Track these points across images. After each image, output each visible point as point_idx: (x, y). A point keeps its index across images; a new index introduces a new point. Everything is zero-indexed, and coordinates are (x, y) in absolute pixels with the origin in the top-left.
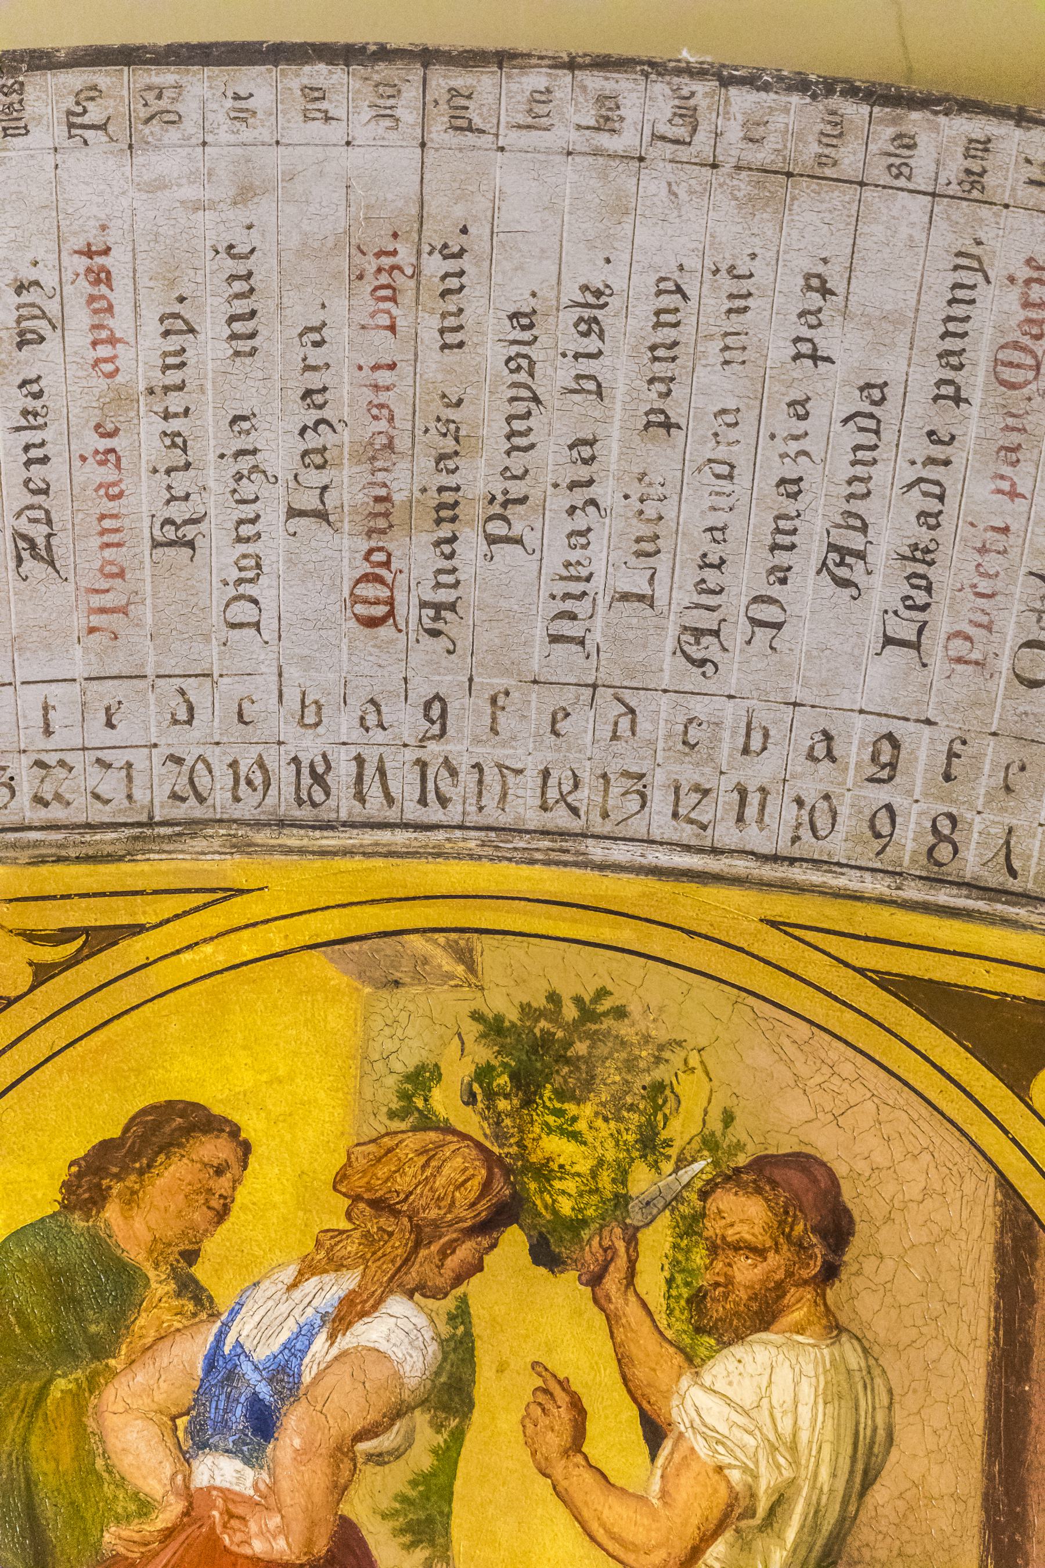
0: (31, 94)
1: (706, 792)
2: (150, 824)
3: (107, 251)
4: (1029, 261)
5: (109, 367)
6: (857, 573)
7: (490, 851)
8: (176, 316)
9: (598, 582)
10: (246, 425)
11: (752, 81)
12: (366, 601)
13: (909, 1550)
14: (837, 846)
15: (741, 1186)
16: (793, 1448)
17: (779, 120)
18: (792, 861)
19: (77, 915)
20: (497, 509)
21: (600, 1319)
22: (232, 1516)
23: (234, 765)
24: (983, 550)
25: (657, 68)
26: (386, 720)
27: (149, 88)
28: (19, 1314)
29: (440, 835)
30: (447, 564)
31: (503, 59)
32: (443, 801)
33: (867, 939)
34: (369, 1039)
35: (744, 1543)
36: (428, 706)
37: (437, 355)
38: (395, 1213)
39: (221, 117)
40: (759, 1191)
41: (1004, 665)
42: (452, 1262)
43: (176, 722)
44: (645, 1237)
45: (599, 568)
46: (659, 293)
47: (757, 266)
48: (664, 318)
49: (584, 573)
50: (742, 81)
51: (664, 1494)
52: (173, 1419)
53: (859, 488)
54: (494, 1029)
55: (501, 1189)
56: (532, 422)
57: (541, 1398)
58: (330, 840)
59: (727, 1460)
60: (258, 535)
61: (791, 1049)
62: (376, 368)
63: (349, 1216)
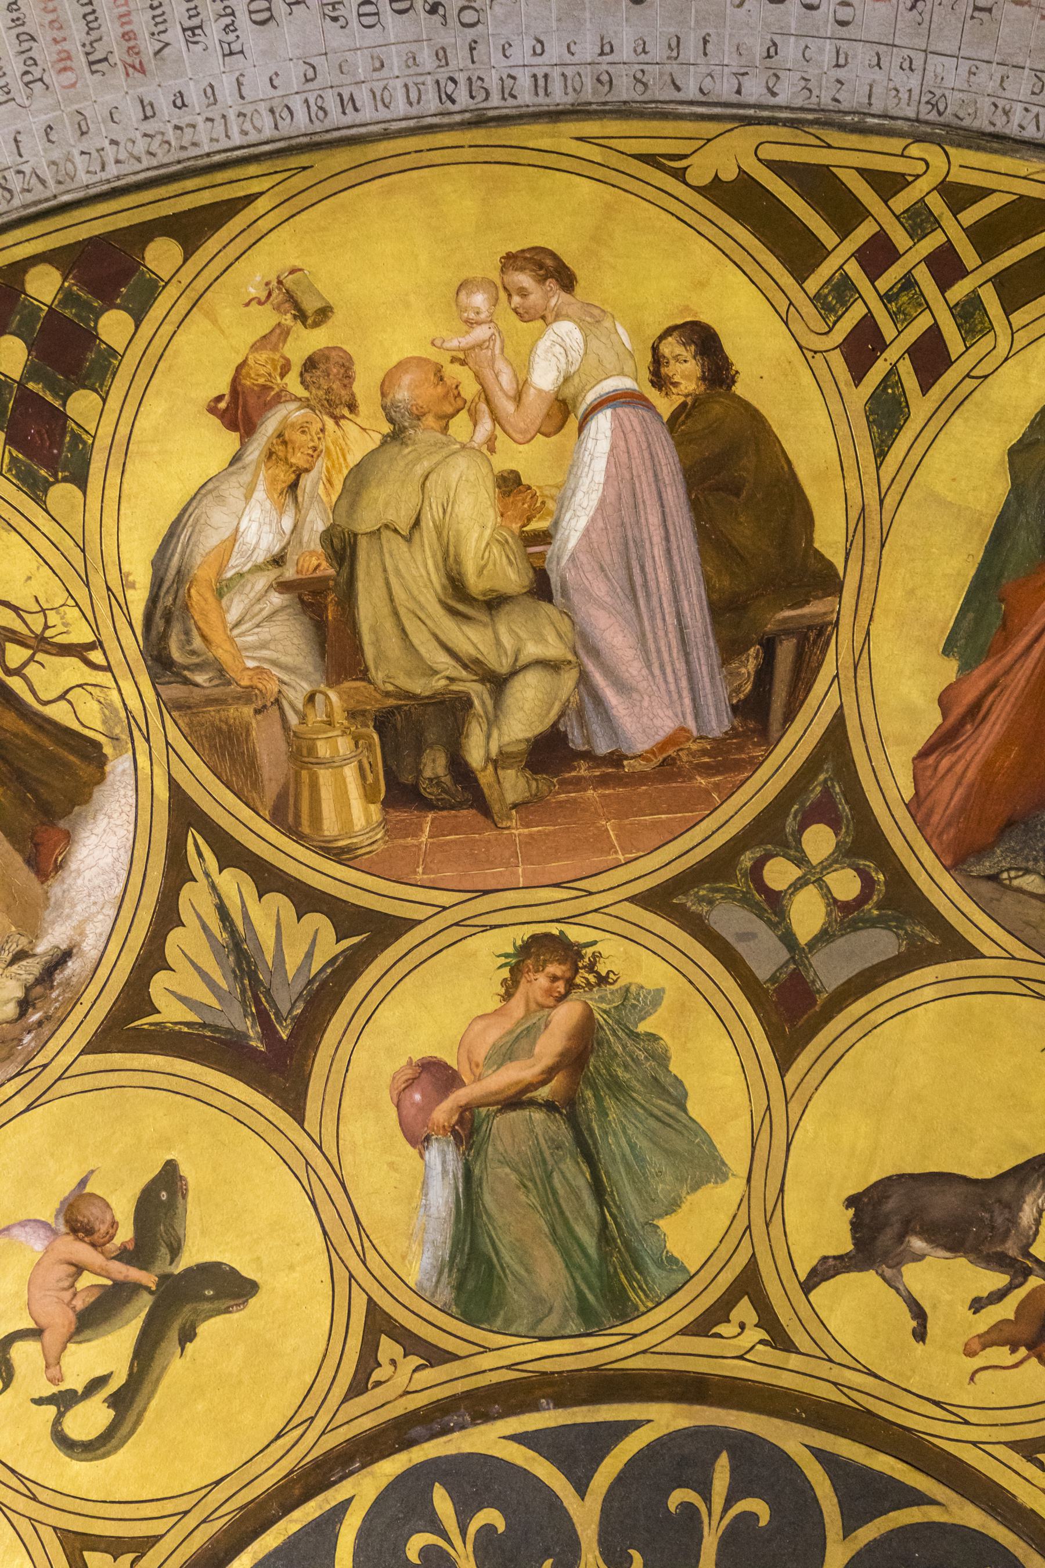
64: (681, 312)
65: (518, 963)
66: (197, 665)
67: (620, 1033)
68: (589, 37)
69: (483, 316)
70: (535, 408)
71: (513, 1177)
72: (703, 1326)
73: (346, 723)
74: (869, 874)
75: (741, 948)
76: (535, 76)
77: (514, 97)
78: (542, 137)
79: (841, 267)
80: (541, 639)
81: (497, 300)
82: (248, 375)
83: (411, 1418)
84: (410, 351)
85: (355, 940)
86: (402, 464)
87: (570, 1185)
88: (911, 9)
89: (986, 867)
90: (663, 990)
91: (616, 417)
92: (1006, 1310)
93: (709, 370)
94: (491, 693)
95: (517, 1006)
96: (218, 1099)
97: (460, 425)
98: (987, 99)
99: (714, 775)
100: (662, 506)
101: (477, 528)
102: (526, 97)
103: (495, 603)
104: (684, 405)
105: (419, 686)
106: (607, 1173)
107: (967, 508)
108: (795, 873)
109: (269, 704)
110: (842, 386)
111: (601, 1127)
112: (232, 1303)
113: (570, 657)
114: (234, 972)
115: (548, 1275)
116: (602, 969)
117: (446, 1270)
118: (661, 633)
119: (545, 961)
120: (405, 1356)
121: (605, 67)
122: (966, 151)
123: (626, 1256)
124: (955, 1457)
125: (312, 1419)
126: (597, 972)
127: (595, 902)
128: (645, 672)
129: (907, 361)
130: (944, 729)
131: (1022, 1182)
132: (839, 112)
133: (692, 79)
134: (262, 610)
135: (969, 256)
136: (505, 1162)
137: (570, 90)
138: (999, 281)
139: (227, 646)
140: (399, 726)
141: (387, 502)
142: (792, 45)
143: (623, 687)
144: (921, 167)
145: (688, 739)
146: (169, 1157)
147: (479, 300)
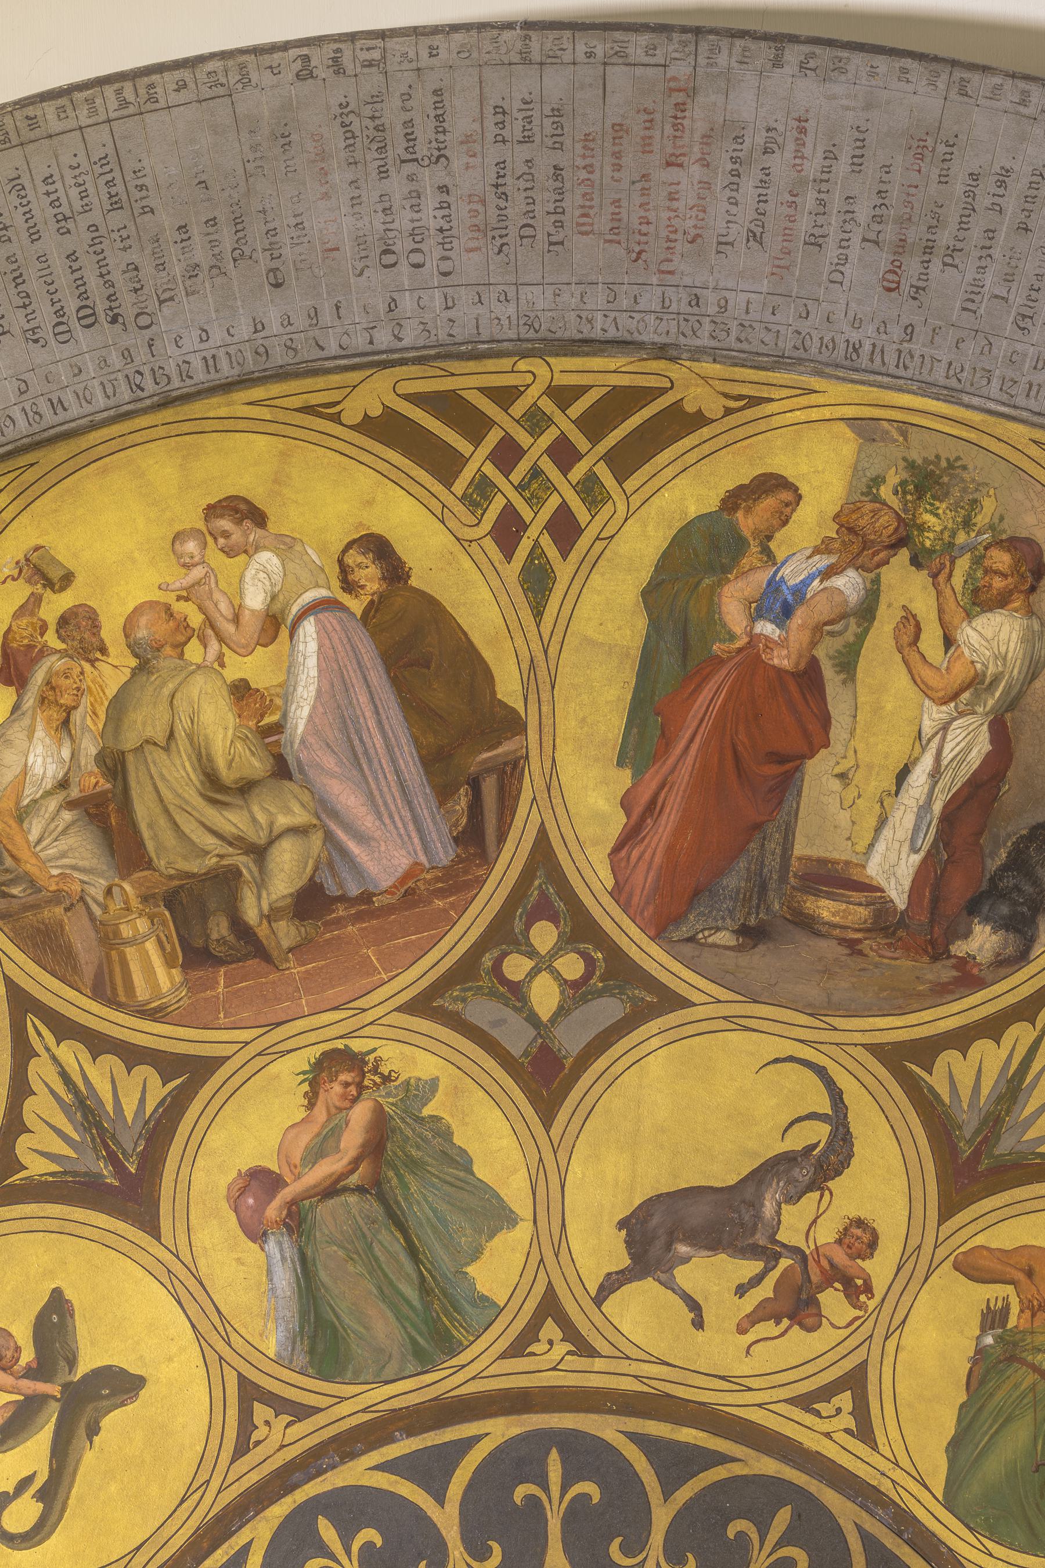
0: (787, 52)
1: (1016, 382)
2: (783, 357)
3: (807, 121)
5: (799, 168)
7: (921, 392)
8: (831, 152)
9: (986, 288)
10: (851, 201)
12: (888, 281)
15: (1002, 548)
16: (1005, 658)
19: (746, 390)
20: (950, 252)
21: (934, 593)
22: (767, 647)
23: (821, 339)
26: (888, 331)
27: (836, 57)
29: (902, 382)
30: (925, 271)
31: (985, 69)
32: (906, 368)
34: (857, 461)
35: (977, 695)
36: (906, 328)
38: (857, 534)
39: (864, 74)
40: (1009, 551)
43: (801, 317)
45: (988, 283)
46: (1033, 175)
48: (1033, 185)
51: (948, 668)
52: (750, 603)
54: (911, 465)
57: (904, 620)
60: (849, 246)
61: (1032, 494)
63: (837, 533)
64: (356, 528)
65: (314, 1078)
66: (11, 880)
68: (243, 320)
69: (196, 559)
70: (251, 626)
72: (518, 1348)
73: (141, 907)
74: (589, 954)
75: (495, 1033)
76: (205, 358)
77: (191, 378)
78: (219, 407)
79: (479, 469)
80: (288, 811)
81: (206, 543)
82: (15, 639)
83: (290, 1467)
84: (142, 597)
85: (179, 1081)
86: (151, 689)
87: (388, 1251)
88: (498, 254)
89: (684, 931)
90: (437, 1078)
91: (318, 621)
92: (766, 1290)
93: (387, 571)
94: (255, 861)
95: (320, 1113)
96: (86, 1231)
97: (194, 652)
98: (572, 313)
99: (447, 897)
100: (368, 687)
101: (221, 730)
102: (200, 376)
103: (246, 788)
104: (372, 602)
105: (195, 867)
106: (417, 1235)
107: (616, 645)
108: (528, 964)
109: (75, 902)
110: (496, 564)
111: (406, 1199)
112: (125, 1397)
113: (315, 821)
114: (82, 1125)
115: (383, 1328)
116: (385, 1070)
117: (298, 1339)
118: (385, 789)
119: (337, 1072)
120: (276, 1417)
121: (261, 342)
122: (563, 359)
123: (445, 1301)
124: (746, 1419)
125: (208, 1481)
126: (380, 1073)
127: (370, 1016)
128: (378, 823)
129: (546, 535)
130: (629, 827)
131: (760, 1182)
132: (455, 344)
133: (332, 339)
134: (57, 826)
135: (581, 443)
136: (332, 1241)
137: (235, 364)
138: (609, 458)
139: (34, 861)
140: (185, 901)
141: (146, 721)
142: (408, 298)
143: (362, 838)
144: (529, 378)
145: (422, 871)
146: (53, 1286)
147: (191, 546)
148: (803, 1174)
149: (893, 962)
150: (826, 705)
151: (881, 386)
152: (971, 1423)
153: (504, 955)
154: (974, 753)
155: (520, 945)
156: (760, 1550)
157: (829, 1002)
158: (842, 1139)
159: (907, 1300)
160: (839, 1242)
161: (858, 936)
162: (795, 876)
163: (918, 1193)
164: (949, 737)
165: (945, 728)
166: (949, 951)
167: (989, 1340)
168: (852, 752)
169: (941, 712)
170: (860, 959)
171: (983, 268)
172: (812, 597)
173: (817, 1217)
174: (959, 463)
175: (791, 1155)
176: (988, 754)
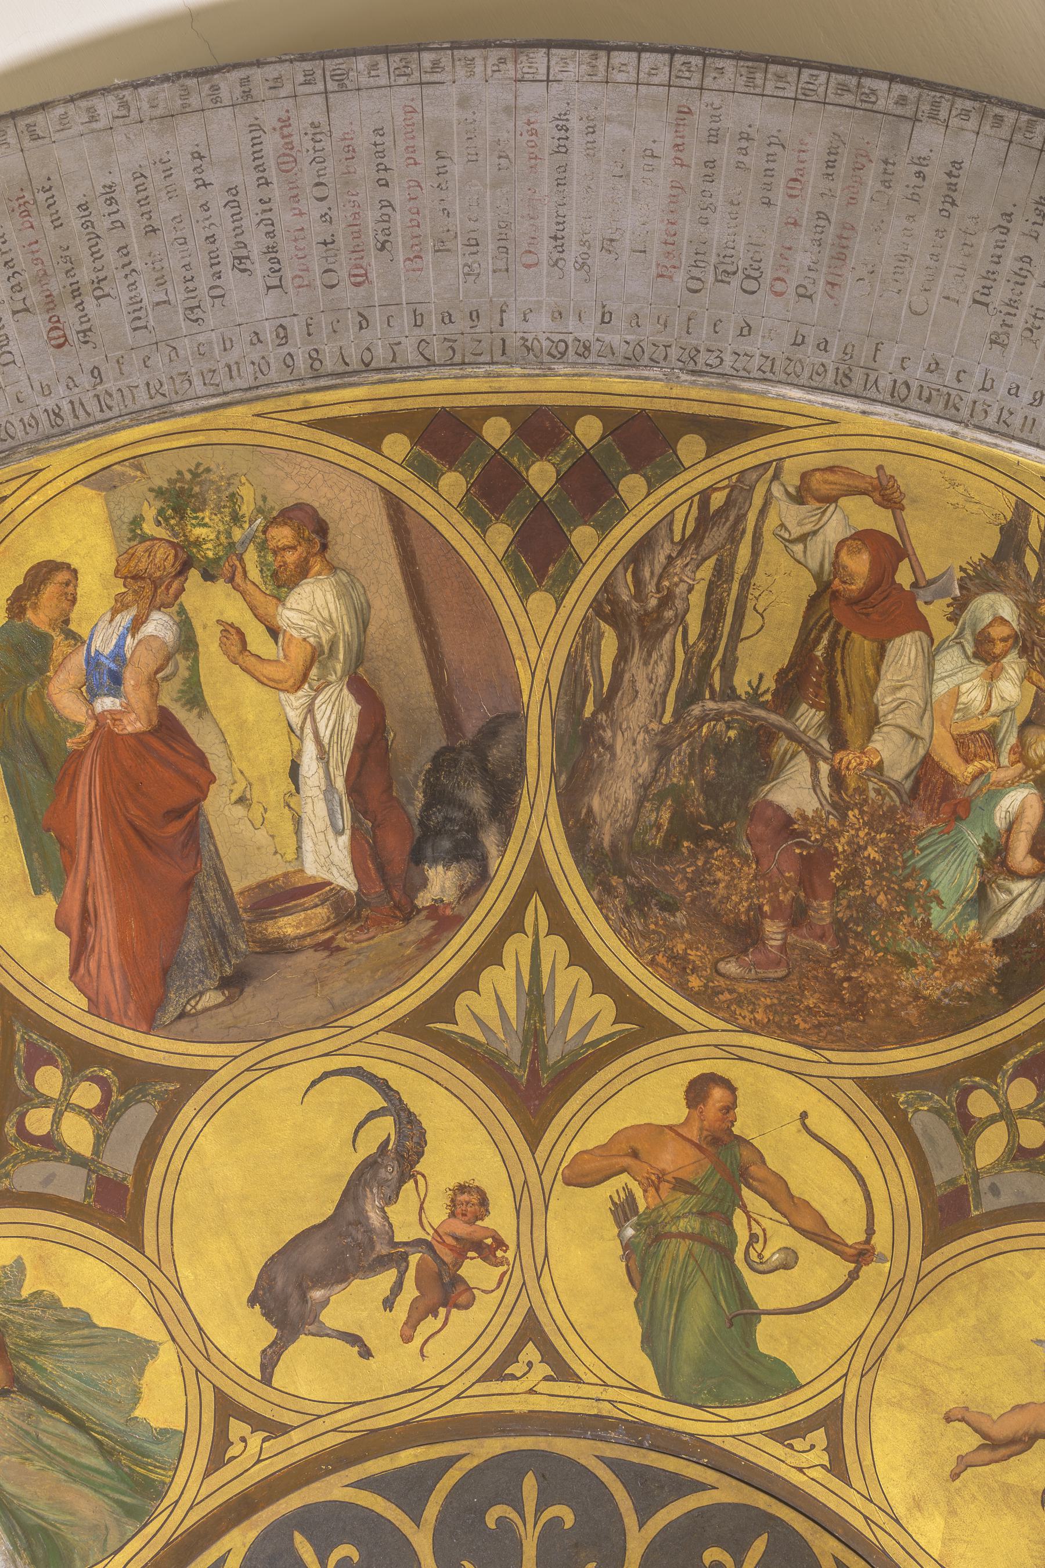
1: (214, 371)
4: (279, 120)
6: (249, 266)
7: (135, 422)
9: (145, 301)
11: (146, 83)
12: (55, 339)
13: (391, 647)
14: (273, 375)
16: (331, 621)
17: (162, 95)
18: (257, 387)
20: (96, 285)
22: (116, 720)
23: (21, 420)
24: (296, 240)
25: (106, 91)
28: (5, 666)
29: (113, 422)
30: (83, 314)
31: (44, 106)
32: (110, 408)
33: (297, 409)
34: (110, 513)
35: (323, 666)
36: (92, 372)
37: (53, 232)
38: (143, 579)
40: (286, 524)
41: (318, 282)
42: (172, 591)
44: (247, 557)
45: (144, 295)
46: (135, 179)
47: (171, 156)
48: (140, 188)
49: (139, 300)
50: (143, 85)
51: (285, 656)
53: (239, 231)
54: (160, 493)
55: (183, 556)
56: (99, 246)
57: (224, 634)
58: (70, 438)
59: (307, 635)
62: (30, 245)
63: (125, 586)
67: (13, 1308)
71: (14, 1459)
72: (217, 1460)
74: (98, 1076)
75: (50, 1190)
87: (56, 1435)
89: (172, 1011)
90: (20, 1258)
92: (410, 1291)
106: (74, 1407)
108: (48, 1113)
111: (47, 1381)
115: (87, 1506)
117: (16, 1556)
123: (129, 1452)
130: (74, 944)
131: (356, 1199)
148: (389, 1172)
149: (371, 942)
150: (194, 744)
151: (96, 436)
152: (652, 1313)
153: (22, 1116)
154: (347, 719)
155: (32, 1100)
156: (525, 1525)
157: (333, 1007)
158: (408, 1123)
159: (539, 1234)
160: (452, 1215)
161: (329, 934)
162: (245, 910)
163: (499, 1135)
164: (318, 717)
165: (310, 710)
166: (416, 907)
167: (630, 1232)
168: (239, 775)
169: (300, 698)
170: (341, 955)
171: (133, 284)
172: (132, 655)
173: (422, 1203)
174: (201, 469)
175: (370, 1160)
176: (360, 713)
